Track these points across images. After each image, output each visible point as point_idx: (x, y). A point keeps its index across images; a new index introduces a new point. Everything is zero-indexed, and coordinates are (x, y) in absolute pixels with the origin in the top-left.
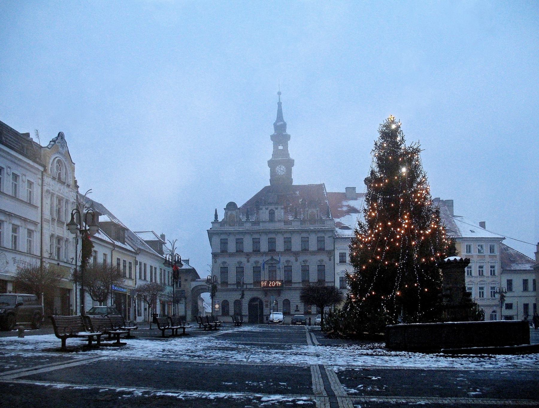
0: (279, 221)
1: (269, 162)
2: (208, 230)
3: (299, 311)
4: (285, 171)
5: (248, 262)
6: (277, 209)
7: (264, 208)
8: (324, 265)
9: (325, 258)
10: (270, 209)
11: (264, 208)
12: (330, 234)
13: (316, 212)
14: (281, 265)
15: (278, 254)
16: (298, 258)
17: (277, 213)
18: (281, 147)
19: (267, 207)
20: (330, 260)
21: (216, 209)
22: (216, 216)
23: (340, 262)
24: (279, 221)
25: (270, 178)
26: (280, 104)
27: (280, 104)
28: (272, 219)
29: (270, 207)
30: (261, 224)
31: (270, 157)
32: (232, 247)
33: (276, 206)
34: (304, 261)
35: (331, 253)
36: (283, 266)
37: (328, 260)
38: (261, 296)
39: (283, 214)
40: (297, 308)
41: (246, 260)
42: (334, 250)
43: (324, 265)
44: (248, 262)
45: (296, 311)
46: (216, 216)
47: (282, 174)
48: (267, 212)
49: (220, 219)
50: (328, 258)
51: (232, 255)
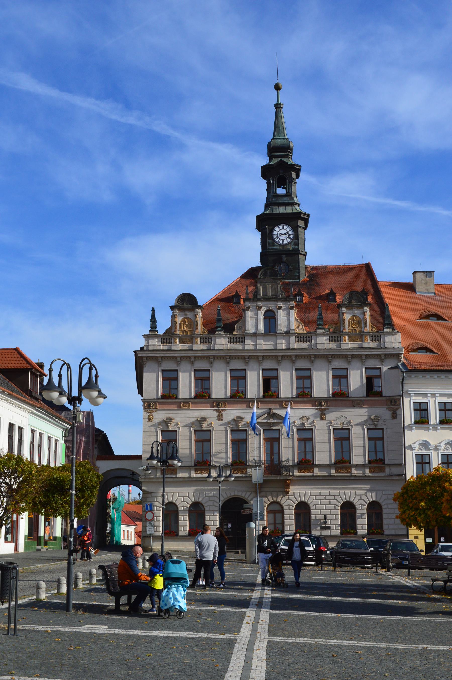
1: (257, 216)
2: (135, 352)
3: (328, 528)
4: (291, 236)
5: (220, 418)
8: (382, 429)
12: (391, 363)
13: (361, 316)
15: (283, 403)
17: (281, 316)
18: (281, 191)
19: (259, 304)
21: (153, 309)
22: (153, 320)
23: (416, 423)
24: (288, 333)
25: (260, 251)
26: (278, 107)
27: (278, 107)
31: (261, 210)
33: (280, 304)
38: (248, 494)
40: (325, 522)
41: (216, 414)
43: (382, 429)
44: (220, 418)
45: (323, 528)
46: (153, 320)
47: (285, 242)
48: (261, 314)
49: (162, 329)
50: (391, 413)
51: (186, 403)
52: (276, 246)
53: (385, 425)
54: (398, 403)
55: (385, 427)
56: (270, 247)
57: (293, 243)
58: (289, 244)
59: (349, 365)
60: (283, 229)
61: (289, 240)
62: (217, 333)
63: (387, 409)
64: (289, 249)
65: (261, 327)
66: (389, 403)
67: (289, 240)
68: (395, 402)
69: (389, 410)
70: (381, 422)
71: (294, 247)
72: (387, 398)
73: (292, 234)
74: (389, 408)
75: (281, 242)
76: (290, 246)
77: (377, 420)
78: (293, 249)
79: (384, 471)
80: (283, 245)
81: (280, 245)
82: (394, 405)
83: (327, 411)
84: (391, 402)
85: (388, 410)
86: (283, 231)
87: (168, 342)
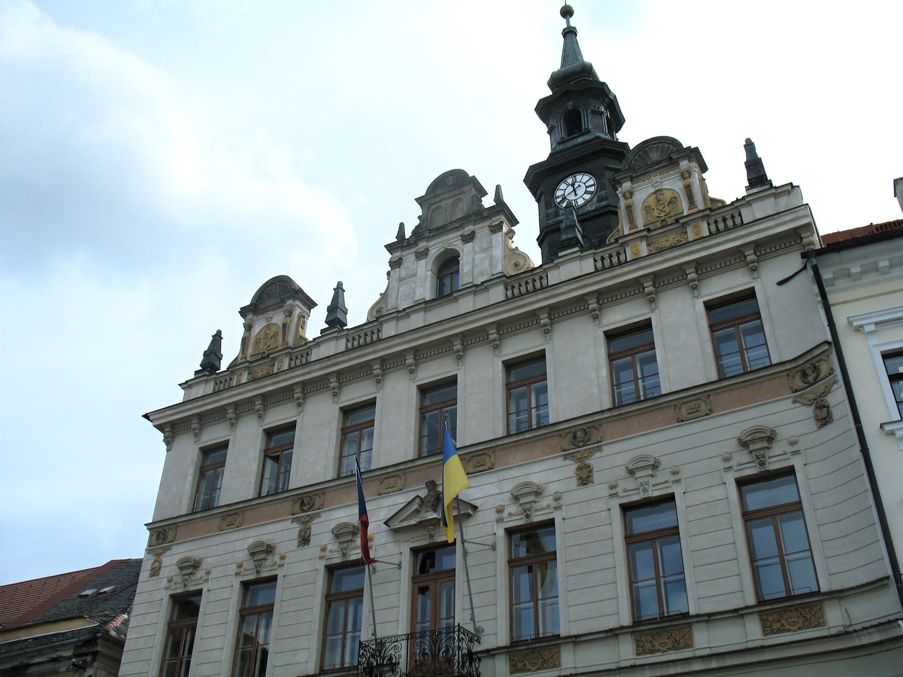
4: (592, 189)
6: (468, 238)
10: (434, 252)
16: (595, 461)
20: (824, 418)
29: (436, 247)
34: (631, 472)
36: (501, 533)
37: (812, 424)
42: (835, 342)
50: (809, 411)
53: (796, 453)
54: (824, 369)
55: (797, 462)
57: (595, 199)
58: (587, 202)
59: (653, 311)
60: (586, 192)
61: (587, 197)
63: (795, 402)
66: (798, 382)
68: (816, 369)
69: (804, 404)
70: (778, 448)
71: (598, 205)
72: (788, 366)
73: (594, 185)
74: (800, 396)
77: (765, 444)
82: (816, 380)
83: (597, 455)
84: (804, 374)
85: (797, 405)
86: (581, 192)
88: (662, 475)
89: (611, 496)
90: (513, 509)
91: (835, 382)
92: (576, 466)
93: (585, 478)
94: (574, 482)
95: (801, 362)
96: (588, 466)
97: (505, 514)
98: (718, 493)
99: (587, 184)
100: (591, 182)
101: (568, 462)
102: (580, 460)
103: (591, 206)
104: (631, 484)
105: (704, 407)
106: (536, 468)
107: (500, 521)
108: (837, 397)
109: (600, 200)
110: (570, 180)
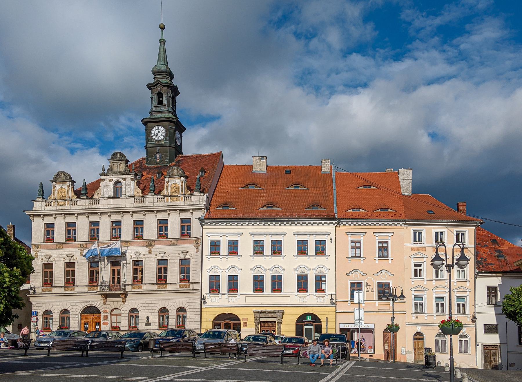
0: (127, 197)
4: (164, 134)
7: (107, 180)
9: (190, 248)
11: (107, 180)
14: (129, 260)
20: (197, 251)
28: (117, 194)
30: (102, 201)
32: (60, 235)
35: (198, 242)
36: (132, 261)
39: (133, 187)
47: (160, 139)
51: (60, 246)
52: (154, 141)
56: (149, 143)
59: (169, 217)
61: (162, 137)
62: (81, 197)
64: (162, 143)
65: (111, 193)
67: (162, 137)
71: (165, 142)
72: (193, 238)
75: (157, 139)
76: (163, 141)
77: (186, 253)
78: (165, 143)
79: (189, 287)
80: (158, 141)
81: (156, 141)
87: (49, 205)
88: (166, 255)
89: (155, 257)
90: (134, 256)
91: (200, 245)
92: (148, 249)
93: (150, 252)
94: (148, 253)
95: (196, 238)
96: (151, 250)
97: (132, 257)
98: (176, 261)
99: (162, 132)
100: (164, 131)
101: (147, 248)
102: (149, 248)
103: (163, 141)
104: (159, 255)
105: (176, 242)
106: (140, 248)
107: (131, 258)
108: (200, 248)
109: (166, 140)
110: (157, 128)
